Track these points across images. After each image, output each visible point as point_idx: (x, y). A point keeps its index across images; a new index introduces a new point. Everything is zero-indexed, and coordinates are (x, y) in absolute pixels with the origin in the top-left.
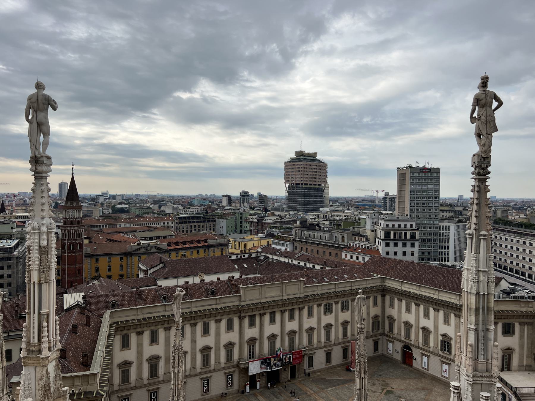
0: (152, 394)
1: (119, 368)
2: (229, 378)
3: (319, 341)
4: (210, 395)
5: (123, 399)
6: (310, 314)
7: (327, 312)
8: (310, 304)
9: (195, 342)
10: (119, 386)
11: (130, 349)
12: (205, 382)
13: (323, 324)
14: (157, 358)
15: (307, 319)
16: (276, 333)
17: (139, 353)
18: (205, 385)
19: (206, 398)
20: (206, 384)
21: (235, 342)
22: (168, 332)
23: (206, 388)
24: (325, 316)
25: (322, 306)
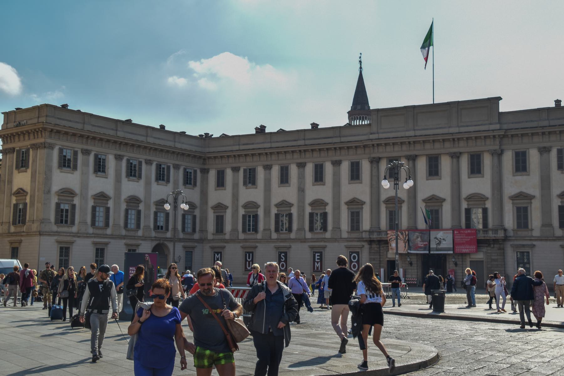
0: (248, 254)
1: (214, 212)
2: (354, 258)
3: (547, 225)
10: (213, 234)
11: (225, 189)
12: (317, 254)
14: (257, 206)
15: (514, 176)
16: (442, 195)
17: (235, 197)
18: (316, 260)
20: (318, 259)
21: (364, 200)
25: (554, 153)
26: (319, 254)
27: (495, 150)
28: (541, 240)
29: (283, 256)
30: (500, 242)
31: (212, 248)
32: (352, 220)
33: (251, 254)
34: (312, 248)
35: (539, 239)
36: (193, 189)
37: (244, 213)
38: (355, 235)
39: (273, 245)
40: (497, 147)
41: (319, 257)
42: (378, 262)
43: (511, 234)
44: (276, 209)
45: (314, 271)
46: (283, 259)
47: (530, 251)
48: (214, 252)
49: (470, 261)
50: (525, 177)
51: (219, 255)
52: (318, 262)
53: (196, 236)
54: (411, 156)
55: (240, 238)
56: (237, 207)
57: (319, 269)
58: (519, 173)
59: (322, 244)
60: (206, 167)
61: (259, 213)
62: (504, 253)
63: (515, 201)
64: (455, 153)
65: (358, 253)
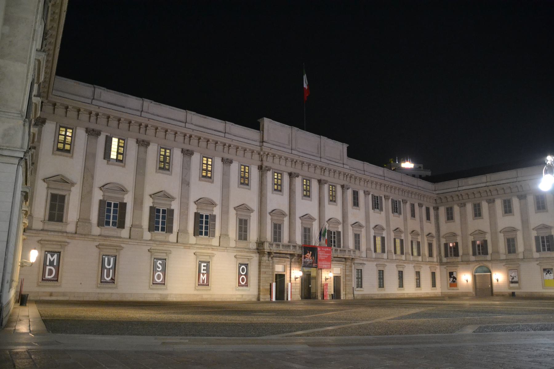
0: (106, 259)
1: (48, 188)
2: (243, 270)
4: (208, 292)
5: (48, 252)
9: (188, 184)
12: (203, 264)
18: (202, 272)
19: (205, 297)
20: (204, 270)
22: (142, 149)
23: (203, 277)
26: (205, 264)
29: (159, 263)
32: (240, 228)
33: (112, 260)
37: (101, 198)
38: (243, 244)
41: (205, 268)
44: (151, 200)
45: (199, 285)
46: (159, 268)
48: (46, 251)
51: (55, 256)
52: (203, 274)
56: (91, 187)
57: (205, 282)
59: (210, 251)
65: (246, 265)
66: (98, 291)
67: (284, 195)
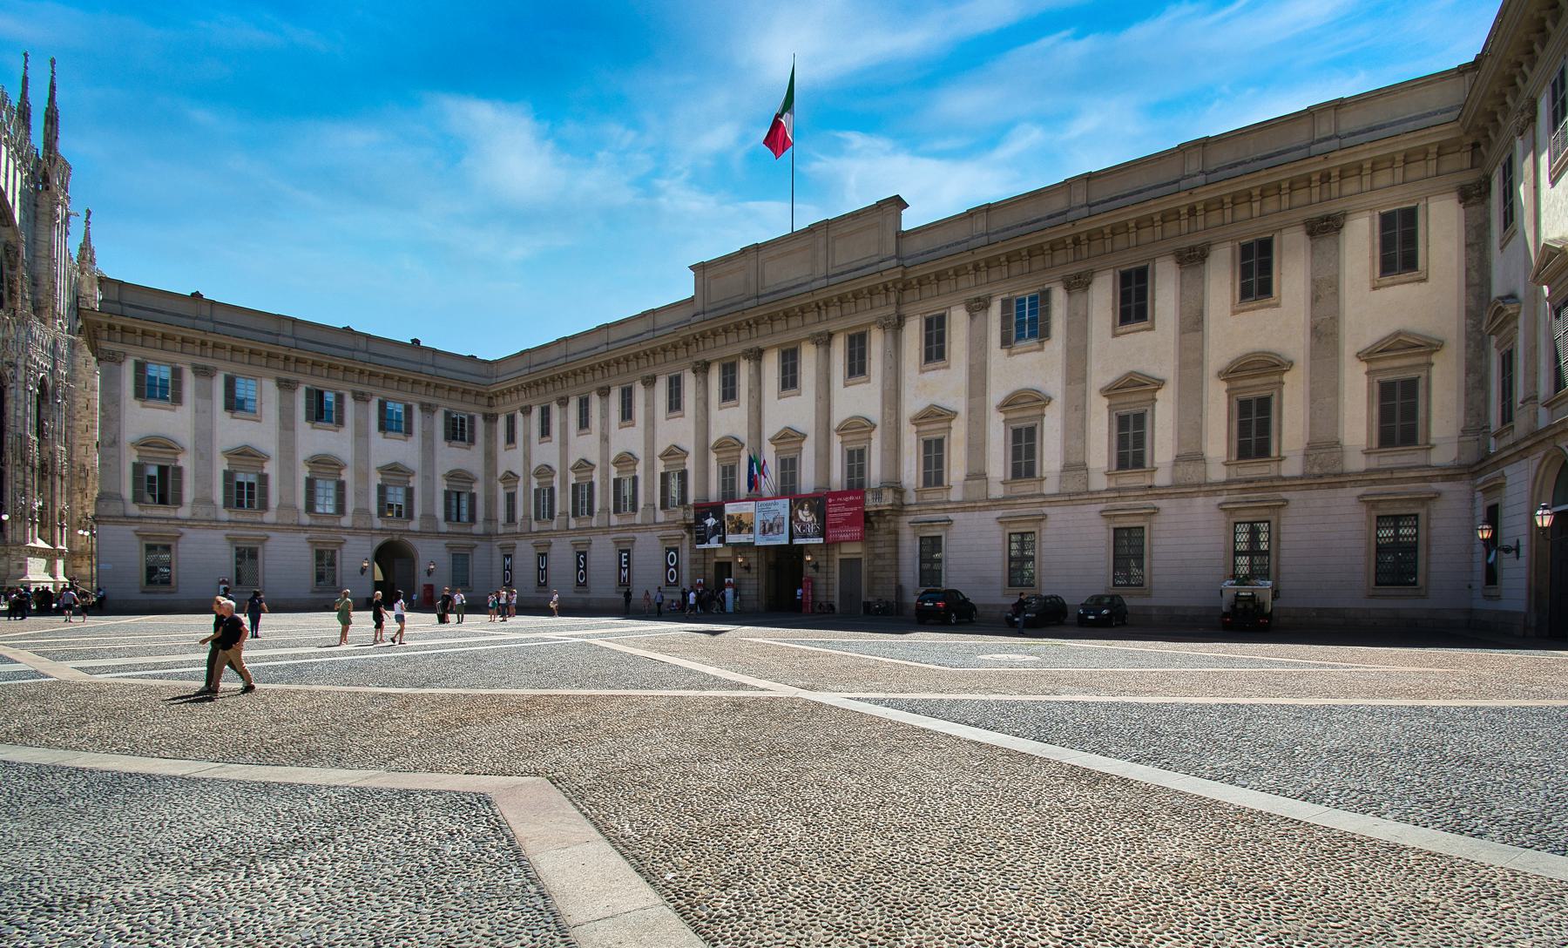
3: (977, 475)
6: (935, 351)
7: (1020, 337)
8: (933, 307)
13: (997, 393)
16: (801, 428)
17: (527, 457)
18: (624, 566)
20: (625, 563)
24: (1010, 355)
27: (887, 318)
28: (964, 509)
30: (888, 518)
31: (502, 548)
34: (617, 542)
35: (963, 507)
36: (469, 449)
39: (569, 540)
40: (891, 310)
42: (701, 566)
43: (911, 498)
47: (943, 534)
49: (841, 560)
50: (942, 372)
53: (478, 528)
54: (751, 351)
55: (533, 530)
58: (931, 366)
60: (494, 411)
61: (554, 485)
62: (897, 541)
63: (922, 428)
64: (819, 334)
65: (676, 550)
66: (538, 595)
67: (741, 404)
